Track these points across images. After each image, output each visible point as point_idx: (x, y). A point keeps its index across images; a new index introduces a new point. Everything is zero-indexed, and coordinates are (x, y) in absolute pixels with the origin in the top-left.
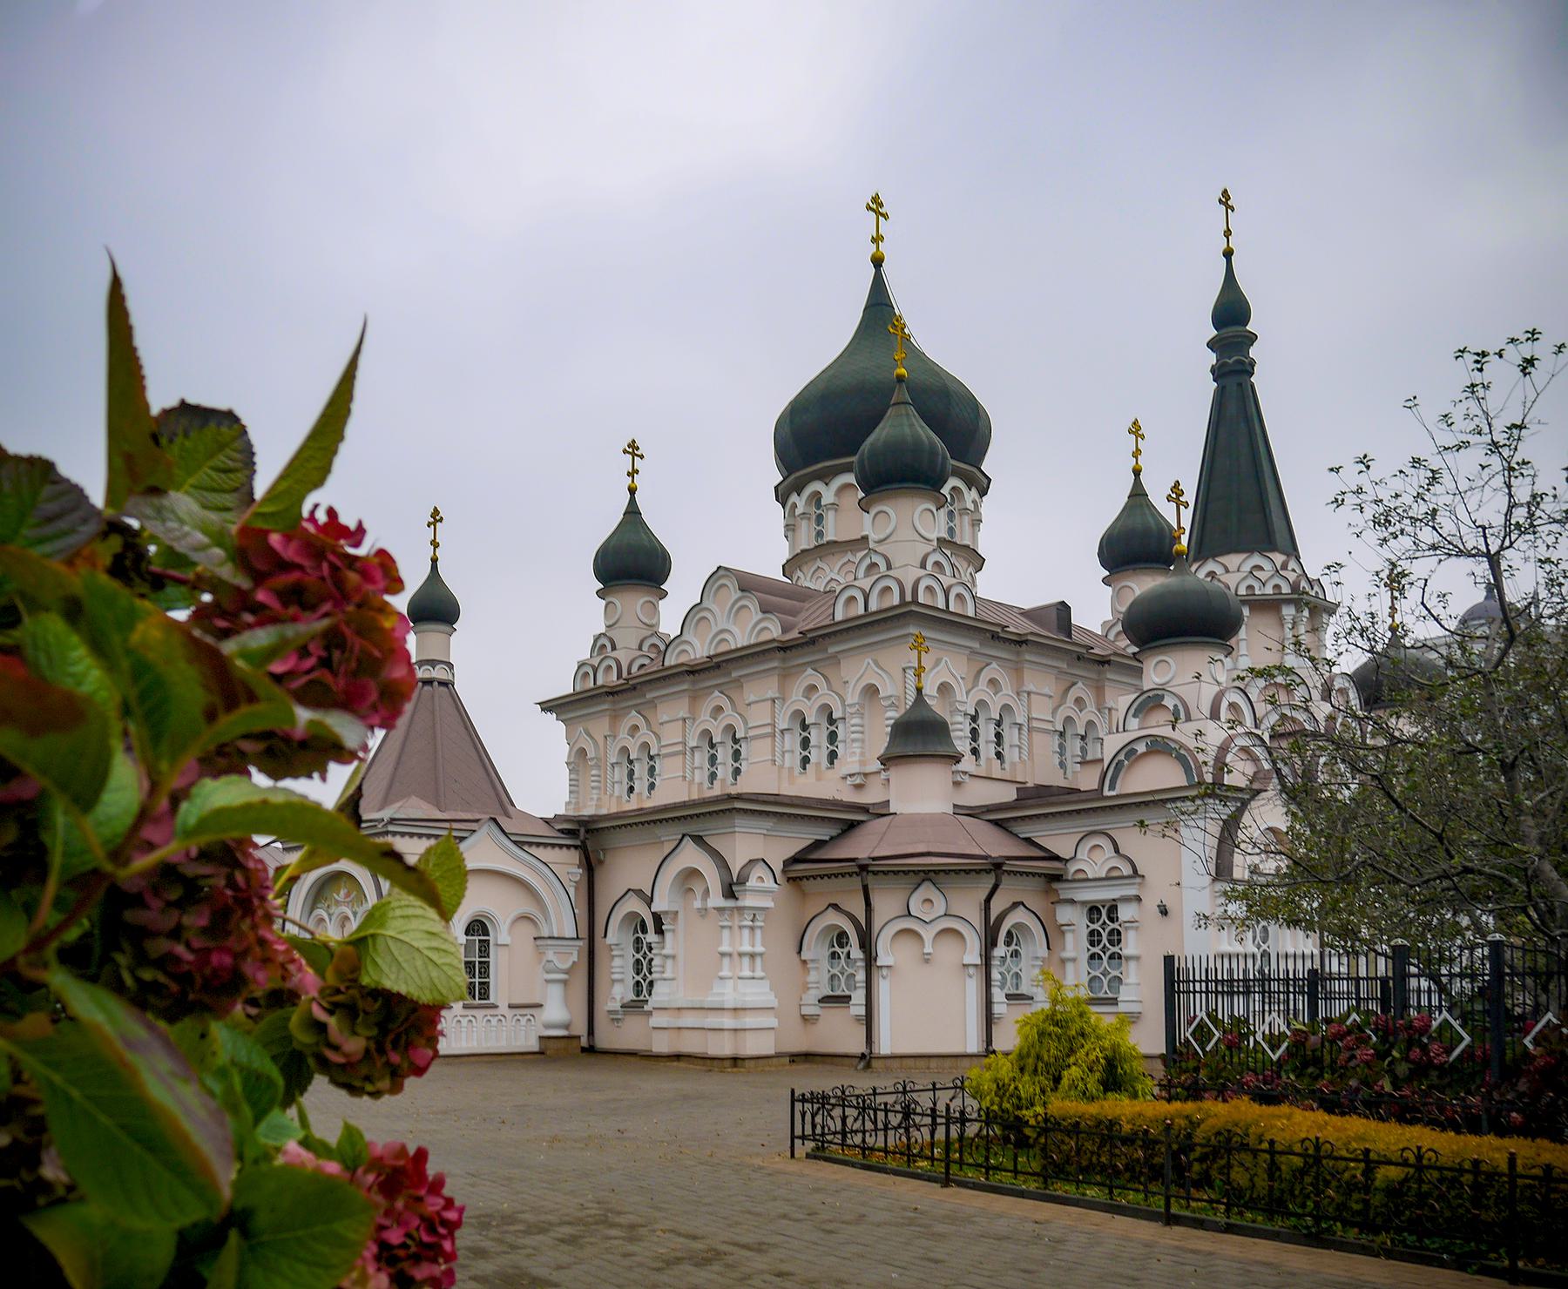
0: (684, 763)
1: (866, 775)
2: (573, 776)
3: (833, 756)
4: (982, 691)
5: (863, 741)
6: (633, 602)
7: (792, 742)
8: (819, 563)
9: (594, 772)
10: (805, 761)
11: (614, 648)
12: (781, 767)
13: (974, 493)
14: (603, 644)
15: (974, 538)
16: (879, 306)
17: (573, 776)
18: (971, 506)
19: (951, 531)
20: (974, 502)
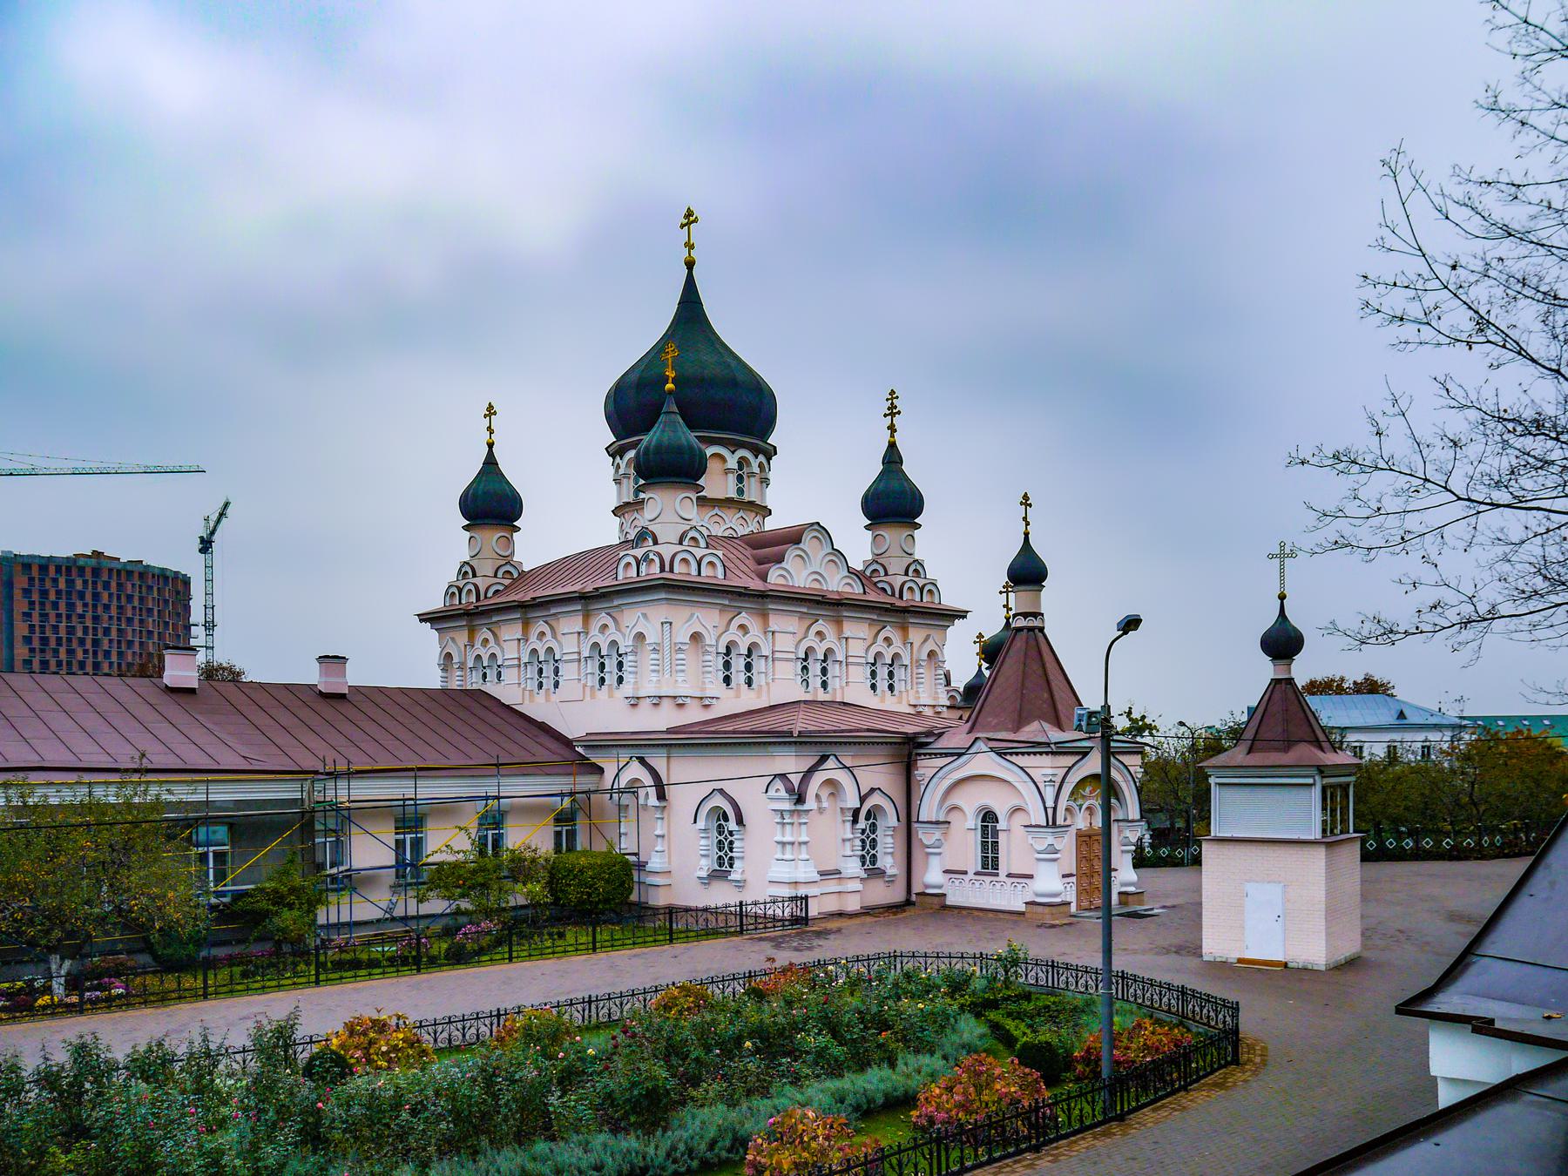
0: (519, 672)
1: (638, 698)
2: (444, 675)
3: (620, 680)
4: (733, 634)
5: (636, 673)
6: (491, 537)
7: (593, 667)
8: (636, 515)
9: (458, 673)
10: (602, 680)
11: (474, 575)
12: (585, 686)
13: (761, 458)
14: (467, 570)
15: (763, 495)
16: (690, 305)
17: (444, 675)
18: (756, 470)
19: (740, 491)
20: (761, 465)
